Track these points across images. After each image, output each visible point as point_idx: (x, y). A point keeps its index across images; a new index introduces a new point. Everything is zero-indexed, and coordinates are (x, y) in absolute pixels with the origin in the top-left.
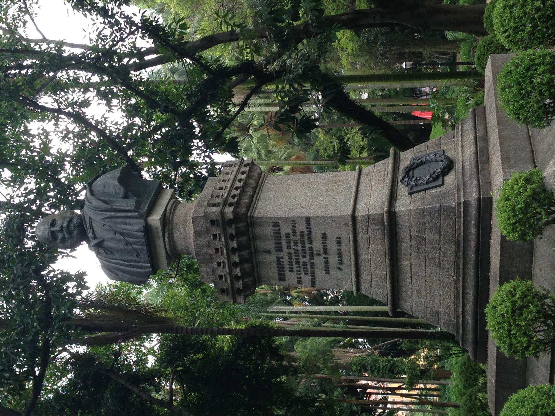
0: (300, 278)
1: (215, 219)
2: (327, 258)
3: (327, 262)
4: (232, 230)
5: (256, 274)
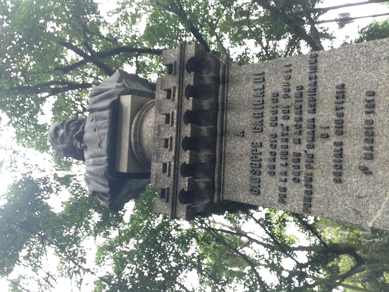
0: (285, 189)
1: (172, 62)
2: (341, 144)
3: (340, 154)
5: (216, 175)
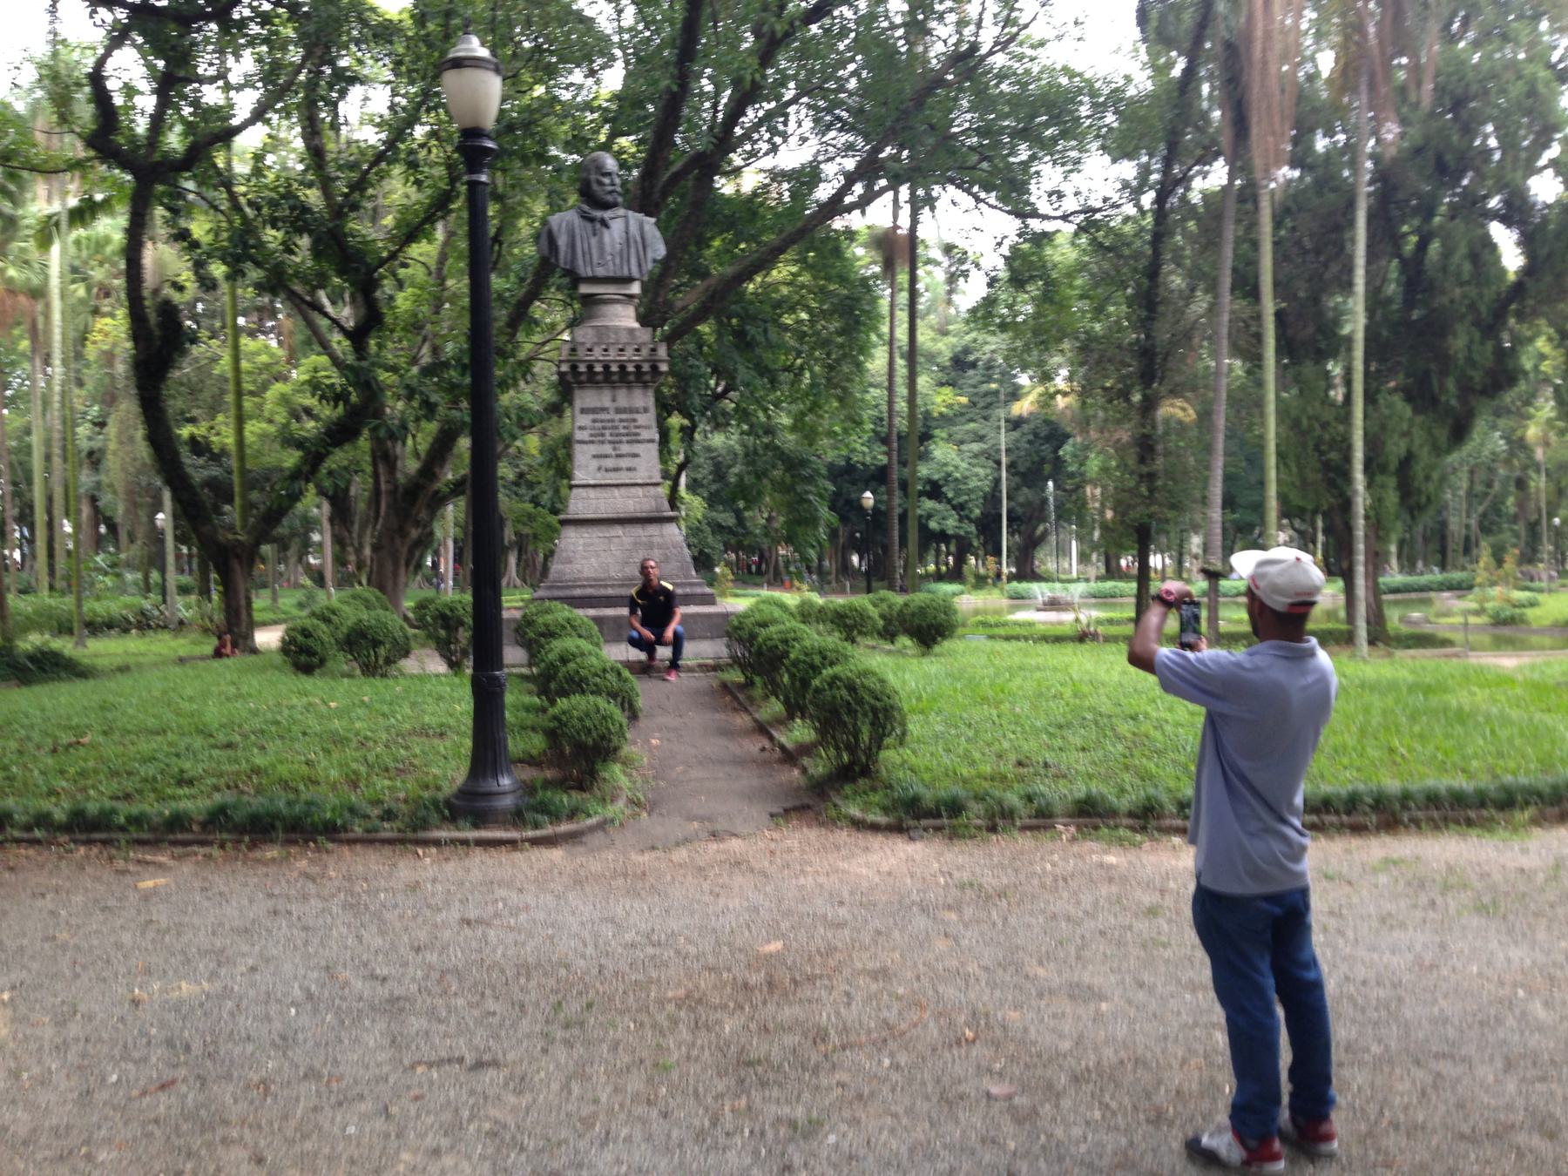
4: (646, 368)
